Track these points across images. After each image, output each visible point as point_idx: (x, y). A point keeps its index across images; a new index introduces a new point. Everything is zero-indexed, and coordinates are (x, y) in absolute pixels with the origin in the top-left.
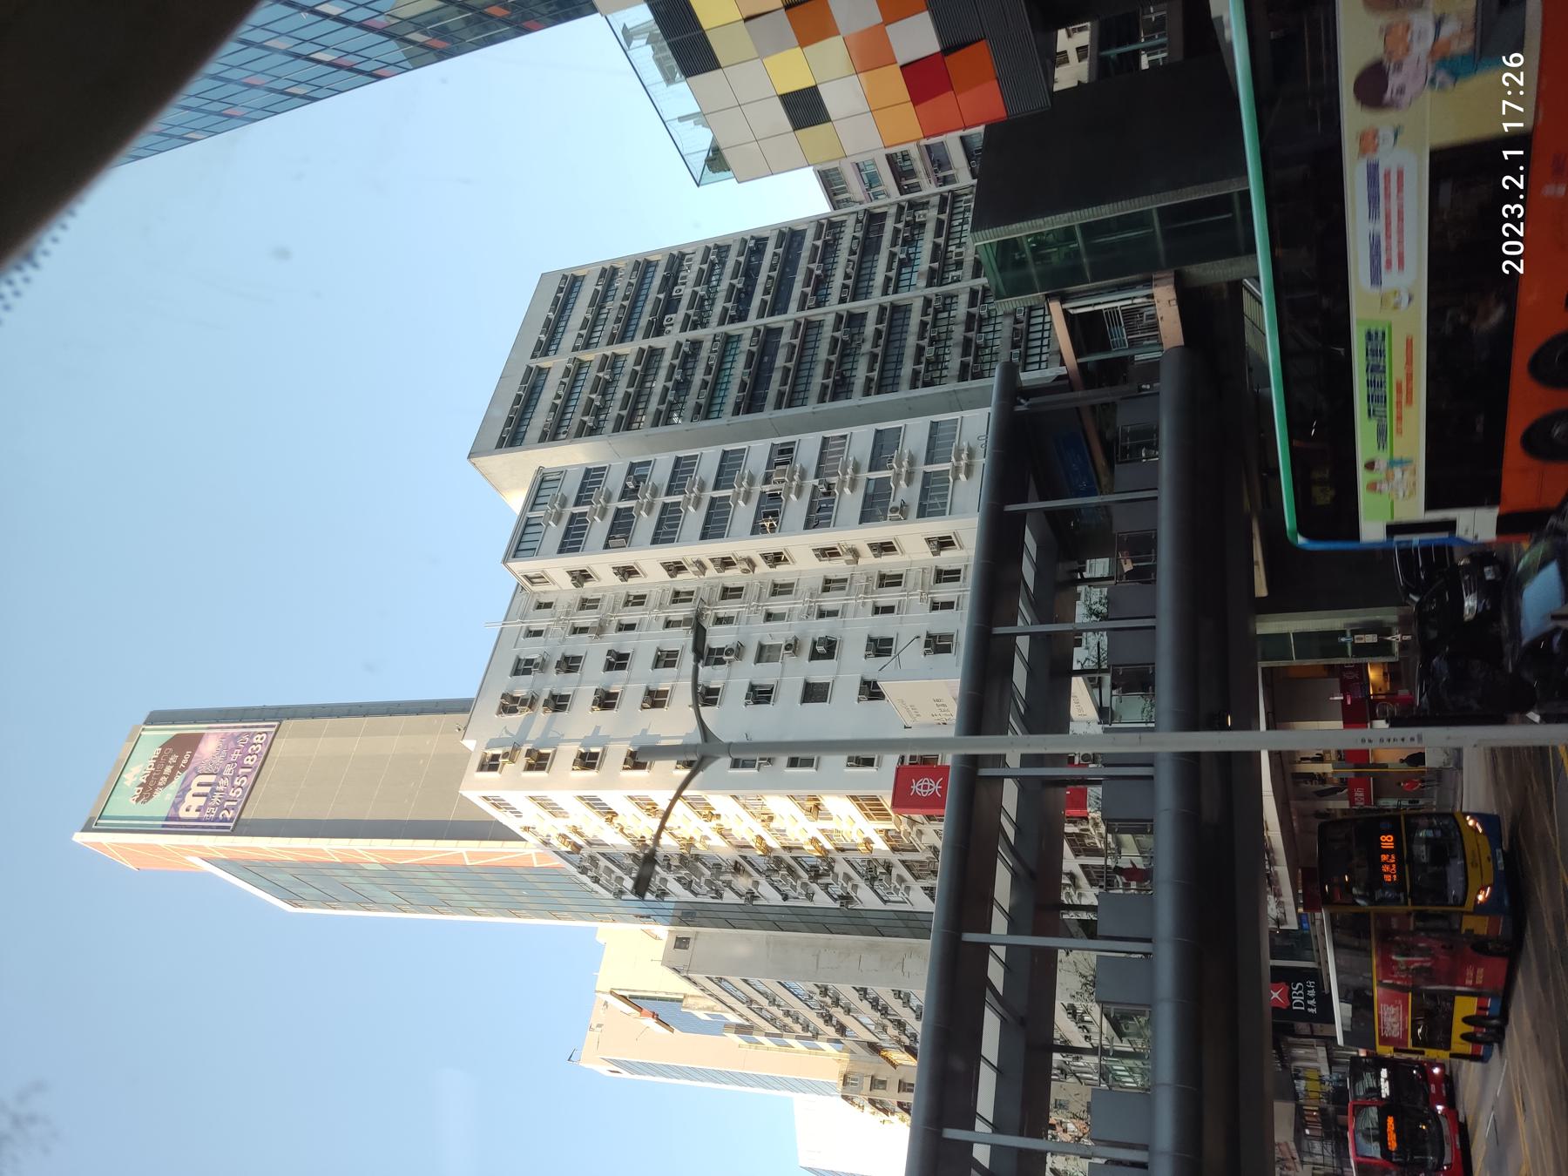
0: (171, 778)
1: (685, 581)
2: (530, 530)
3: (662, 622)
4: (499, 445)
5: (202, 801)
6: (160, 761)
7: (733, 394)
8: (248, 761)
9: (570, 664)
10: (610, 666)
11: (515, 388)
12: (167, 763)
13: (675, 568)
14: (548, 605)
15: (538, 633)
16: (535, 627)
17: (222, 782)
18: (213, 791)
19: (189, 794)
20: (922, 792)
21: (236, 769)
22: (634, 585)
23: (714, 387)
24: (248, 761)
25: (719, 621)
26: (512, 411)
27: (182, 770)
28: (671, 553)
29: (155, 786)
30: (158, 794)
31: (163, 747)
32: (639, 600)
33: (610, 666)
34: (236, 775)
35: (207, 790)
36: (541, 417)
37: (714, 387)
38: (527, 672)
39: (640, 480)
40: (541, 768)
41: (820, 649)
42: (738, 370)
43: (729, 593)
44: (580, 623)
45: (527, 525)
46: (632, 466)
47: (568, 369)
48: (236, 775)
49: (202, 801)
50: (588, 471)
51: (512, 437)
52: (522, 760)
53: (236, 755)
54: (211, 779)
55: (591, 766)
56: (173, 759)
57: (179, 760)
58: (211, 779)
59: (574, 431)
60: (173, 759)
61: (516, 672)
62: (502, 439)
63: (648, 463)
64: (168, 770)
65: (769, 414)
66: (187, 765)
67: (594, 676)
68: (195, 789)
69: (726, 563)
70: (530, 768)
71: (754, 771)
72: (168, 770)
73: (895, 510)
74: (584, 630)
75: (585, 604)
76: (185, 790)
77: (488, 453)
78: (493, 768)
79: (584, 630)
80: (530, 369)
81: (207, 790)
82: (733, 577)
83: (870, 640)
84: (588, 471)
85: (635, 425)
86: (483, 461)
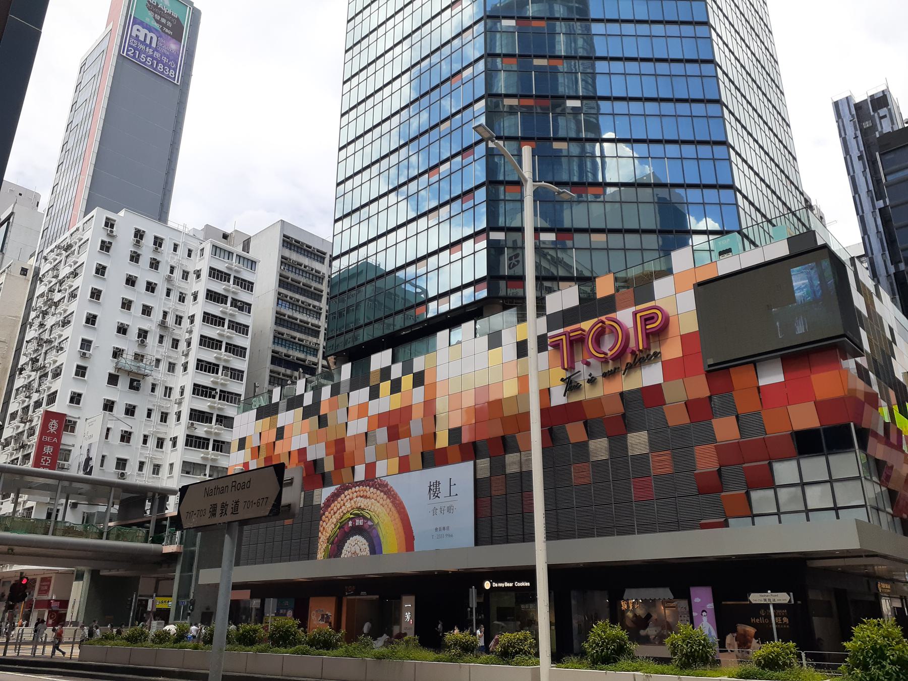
0: (158, 22)
1: (186, 322)
2: (227, 254)
3: (167, 310)
4: (284, 236)
5: (142, 38)
6: (169, 17)
7: (283, 350)
8: (160, 66)
9: (155, 264)
10: (149, 283)
11: (316, 245)
12: (167, 20)
13: (192, 319)
14: (189, 255)
15: (175, 250)
16: (179, 249)
17: (151, 50)
18: (146, 45)
19: (147, 32)
20: (51, 424)
21: (156, 59)
22: (189, 298)
23: (291, 343)
24: (160, 66)
25: (161, 337)
26: (303, 244)
27: (162, 29)
28: (199, 319)
29: (155, 13)
30: (150, 14)
31: (178, 19)
32: (182, 299)
33: (149, 283)
34: (153, 59)
35: (148, 42)
36: (294, 256)
37: (291, 343)
38: (155, 244)
39: (241, 309)
40: (102, 248)
41: (135, 383)
42: (296, 354)
43: (175, 343)
44: (175, 271)
45: (229, 252)
46: (250, 305)
47: (319, 272)
48: (153, 59)
49: (142, 38)
50: (253, 284)
51: (288, 242)
52: (107, 239)
53: (165, 60)
54: (154, 45)
55: (97, 272)
56: (169, 24)
57: (168, 28)
58: (154, 45)
59: (284, 273)
60: (169, 24)
61: (156, 238)
62: (288, 238)
63: (249, 312)
64: (164, 21)
65: (268, 365)
66: (164, 32)
67: (144, 274)
68: (150, 35)
69: (189, 344)
70: (103, 242)
71: (79, 349)
72: (164, 21)
73: (192, 424)
74: (172, 272)
75: (185, 275)
76: (150, 29)
77: (282, 228)
78: (106, 225)
79: (172, 272)
80: (325, 254)
81: (148, 42)
82: (182, 346)
83: (134, 407)
84: (253, 284)
85: (280, 302)
86: (279, 227)
